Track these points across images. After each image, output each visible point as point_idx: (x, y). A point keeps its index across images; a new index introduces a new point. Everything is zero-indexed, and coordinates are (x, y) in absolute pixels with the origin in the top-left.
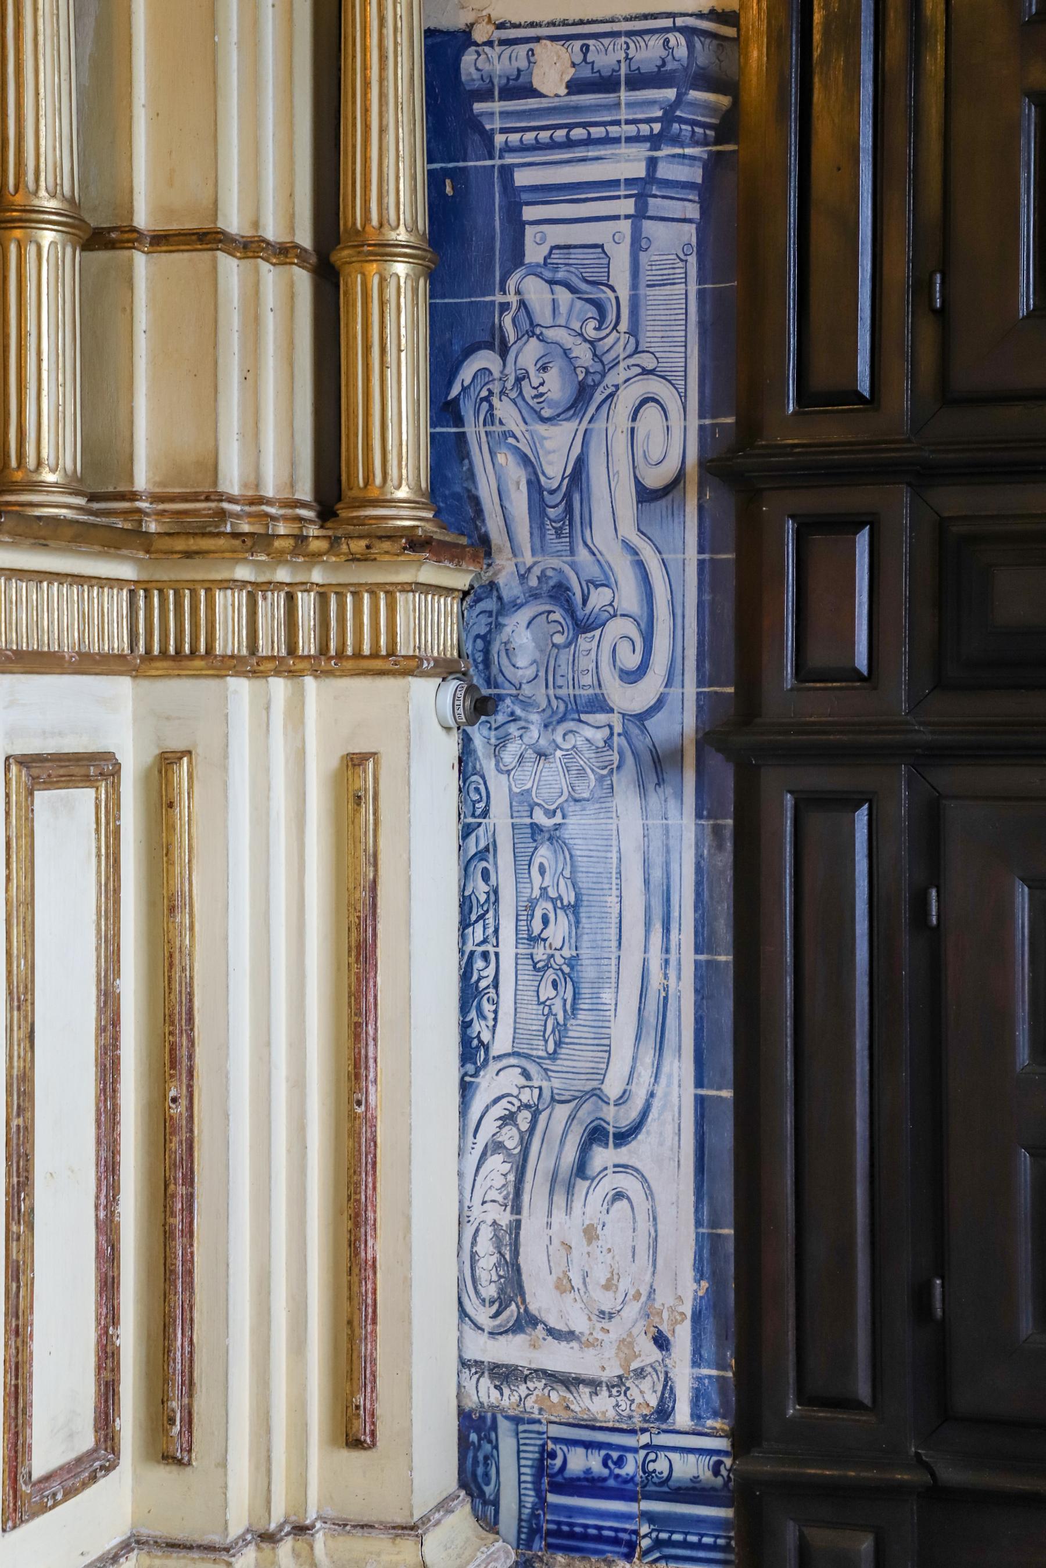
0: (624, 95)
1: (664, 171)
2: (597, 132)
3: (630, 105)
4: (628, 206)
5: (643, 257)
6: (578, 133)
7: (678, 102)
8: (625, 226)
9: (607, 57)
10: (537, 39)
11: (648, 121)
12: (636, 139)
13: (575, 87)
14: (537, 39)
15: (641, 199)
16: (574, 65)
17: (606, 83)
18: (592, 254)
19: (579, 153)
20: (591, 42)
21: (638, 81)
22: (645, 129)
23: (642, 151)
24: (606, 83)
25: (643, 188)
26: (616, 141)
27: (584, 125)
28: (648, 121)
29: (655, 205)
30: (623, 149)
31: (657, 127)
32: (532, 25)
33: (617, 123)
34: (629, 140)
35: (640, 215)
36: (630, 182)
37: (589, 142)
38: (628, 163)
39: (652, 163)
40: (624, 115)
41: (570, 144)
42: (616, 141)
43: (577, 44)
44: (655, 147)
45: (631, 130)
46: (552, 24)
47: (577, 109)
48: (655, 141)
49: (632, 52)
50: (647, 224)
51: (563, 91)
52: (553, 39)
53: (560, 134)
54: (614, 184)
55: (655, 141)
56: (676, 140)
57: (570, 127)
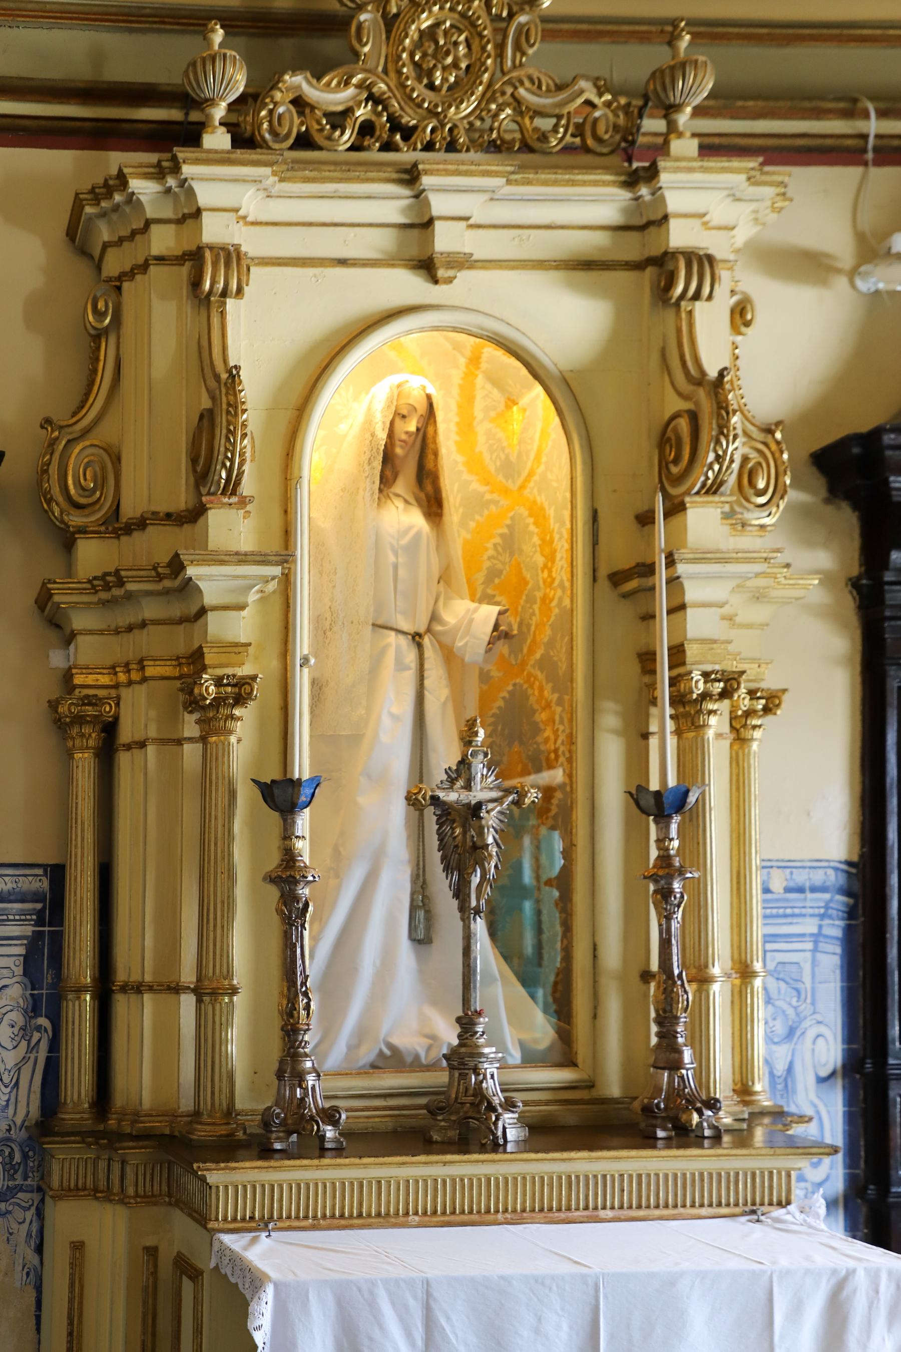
0: (809, 895)
1: (827, 931)
2: (797, 911)
3: (811, 900)
4: (809, 946)
5: (817, 969)
6: (789, 911)
7: (831, 900)
8: (809, 955)
9: (801, 877)
10: (772, 867)
11: (819, 907)
12: (812, 915)
13: (788, 890)
14: (772, 867)
15: (816, 943)
16: (786, 880)
17: (800, 890)
18: (794, 968)
19: (789, 920)
20: (794, 870)
21: (813, 890)
22: (817, 911)
23: (816, 921)
24: (800, 890)
25: (817, 938)
26: (804, 915)
27: (792, 907)
28: (819, 907)
29: (822, 946)
30: (808, 920)
31: (822, 911)
32: (770, 860)
33: (804, 907)
34: (812, 915)
35: (815, 950)
36: (812, 935)
37: (793, 915)
38: (810, 926)
39: (820, 927)
40: (808, 904)
41: (785, 916)
42: (804, 915)
43: (788, 871)
44: (822, 920)
45: (810, 911)
46: (777, 861)
47: (787, 900)
48: (822, 917)
49: (811, 876)
50: (818, 955)
51: (782, 891)
52: (779, 867)
53: (781, 911)
54: (803, 935)
55: (822, 917)
56: (830, 917)
57: (785, 908)
